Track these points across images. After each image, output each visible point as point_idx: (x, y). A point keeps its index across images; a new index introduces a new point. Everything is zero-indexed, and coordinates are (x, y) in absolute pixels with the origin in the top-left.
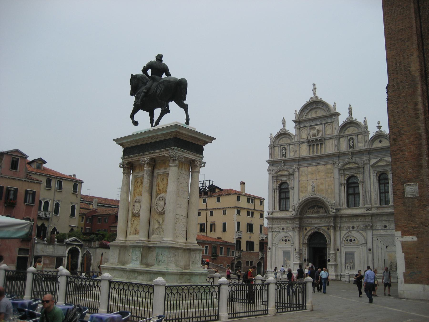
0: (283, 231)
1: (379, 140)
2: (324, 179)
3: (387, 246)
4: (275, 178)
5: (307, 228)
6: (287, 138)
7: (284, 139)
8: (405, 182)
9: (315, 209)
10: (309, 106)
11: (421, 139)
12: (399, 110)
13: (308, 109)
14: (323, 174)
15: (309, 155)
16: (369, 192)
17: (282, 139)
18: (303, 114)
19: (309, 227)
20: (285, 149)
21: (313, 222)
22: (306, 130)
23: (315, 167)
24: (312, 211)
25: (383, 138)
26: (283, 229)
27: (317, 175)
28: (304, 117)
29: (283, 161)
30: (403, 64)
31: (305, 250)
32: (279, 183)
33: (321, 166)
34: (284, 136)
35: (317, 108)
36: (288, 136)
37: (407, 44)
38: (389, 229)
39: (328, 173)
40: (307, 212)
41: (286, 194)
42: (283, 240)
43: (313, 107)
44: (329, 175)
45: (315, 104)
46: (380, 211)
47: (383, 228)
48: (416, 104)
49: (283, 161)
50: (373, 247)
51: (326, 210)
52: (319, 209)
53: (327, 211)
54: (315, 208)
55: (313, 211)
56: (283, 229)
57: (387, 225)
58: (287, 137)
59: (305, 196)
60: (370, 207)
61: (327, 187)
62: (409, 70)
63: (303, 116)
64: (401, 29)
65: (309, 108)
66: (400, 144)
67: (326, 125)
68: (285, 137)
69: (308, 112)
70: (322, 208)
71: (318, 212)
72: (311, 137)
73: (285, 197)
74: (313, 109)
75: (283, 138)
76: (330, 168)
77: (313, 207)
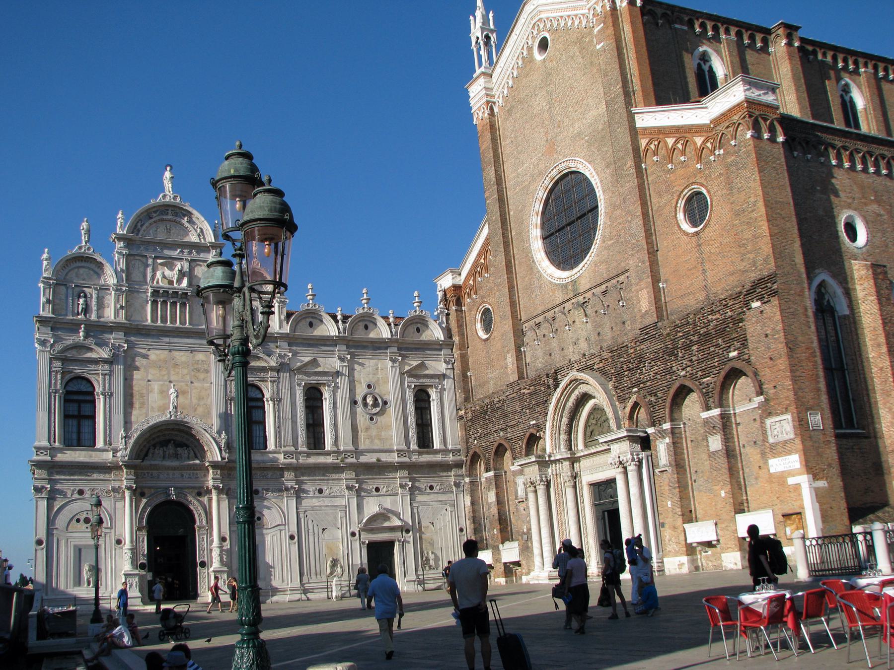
0: (81, 497)
1: (308, 320)
2: (189, 383)
3: (324, 530)
4: (58, 364)
5: (146, 491)
6: (92, 272)
7: (82, 271)
8: (807, 409)
9: (171, 449)
10: (155, 212)
11: (815, 356)
12: (791, 310)
13: (151, 218)
14: (185, 371)
15: (115, 318)
16: (290, 422)
17: (76, 270)
18: (139, 225)
19: (150, 488)
20: (85, 296)
21: (161, 476)
22: (143, 263)
23: (166, 352)
24: (161, 453)
25: (316, 318)
26: (81, 492)
27: (172, 372)
28: (141, 233)
29: (83, 326)
30: (787, 251)
31: (143, 542)
32: (68, 377)
33: (182, 353)
34: (83, 264)
35: (175, 221)
36: (93, 266)
37: (788, 224)
38: (329, 496)
39: (199, 371)
40: (150, 455)
41: (79, 407)
42: (78, 521)
43: (165, 217)
44: (202, 376)
45: (170, 212)
46: (586, 453)
47: (317, 494)
48: (806, 310)
49: (83, 326)
50: (298, 532)
51: (197, 452)
52: (179, 449)
53: (199, 455)
54: (170, 446)
55: (164, 452)
56: (81, 492)
57: (324, 488)
58: (89, 269)
59: (156, 418)
60: (293, 452)
61: (195, 401)
62: (793, 261)
63: (139, 231)
64: (780, 202)
65: (154, 215)
66: (798, 358)
67: (193, 264)
68: (83, 267)
69: (151, 224)
70: (187, 446)
71: (177, 456)
72: (158, 282)
73: (76, 413)
74: (162, 220)
75: (79, 267)
76: (203, 361)
77: (165, 443)
